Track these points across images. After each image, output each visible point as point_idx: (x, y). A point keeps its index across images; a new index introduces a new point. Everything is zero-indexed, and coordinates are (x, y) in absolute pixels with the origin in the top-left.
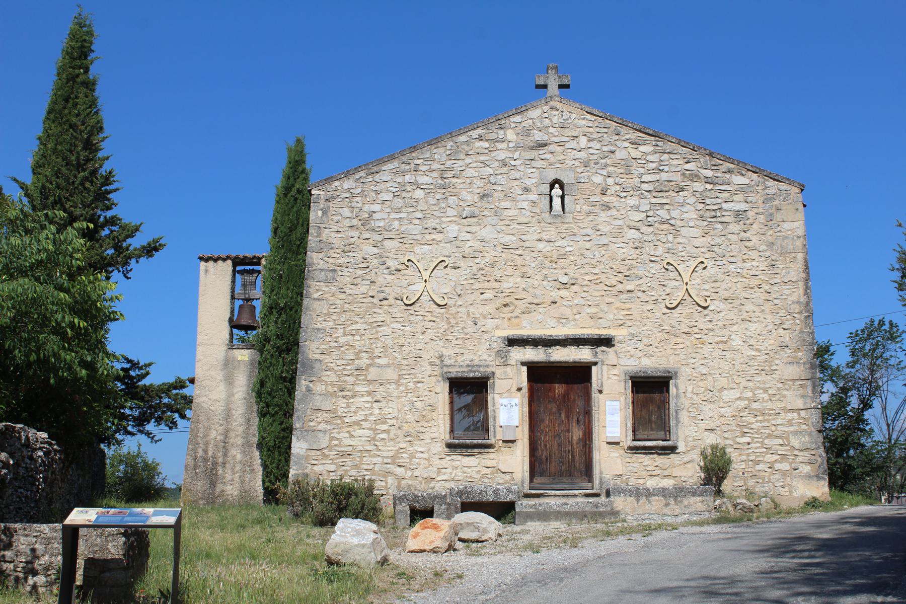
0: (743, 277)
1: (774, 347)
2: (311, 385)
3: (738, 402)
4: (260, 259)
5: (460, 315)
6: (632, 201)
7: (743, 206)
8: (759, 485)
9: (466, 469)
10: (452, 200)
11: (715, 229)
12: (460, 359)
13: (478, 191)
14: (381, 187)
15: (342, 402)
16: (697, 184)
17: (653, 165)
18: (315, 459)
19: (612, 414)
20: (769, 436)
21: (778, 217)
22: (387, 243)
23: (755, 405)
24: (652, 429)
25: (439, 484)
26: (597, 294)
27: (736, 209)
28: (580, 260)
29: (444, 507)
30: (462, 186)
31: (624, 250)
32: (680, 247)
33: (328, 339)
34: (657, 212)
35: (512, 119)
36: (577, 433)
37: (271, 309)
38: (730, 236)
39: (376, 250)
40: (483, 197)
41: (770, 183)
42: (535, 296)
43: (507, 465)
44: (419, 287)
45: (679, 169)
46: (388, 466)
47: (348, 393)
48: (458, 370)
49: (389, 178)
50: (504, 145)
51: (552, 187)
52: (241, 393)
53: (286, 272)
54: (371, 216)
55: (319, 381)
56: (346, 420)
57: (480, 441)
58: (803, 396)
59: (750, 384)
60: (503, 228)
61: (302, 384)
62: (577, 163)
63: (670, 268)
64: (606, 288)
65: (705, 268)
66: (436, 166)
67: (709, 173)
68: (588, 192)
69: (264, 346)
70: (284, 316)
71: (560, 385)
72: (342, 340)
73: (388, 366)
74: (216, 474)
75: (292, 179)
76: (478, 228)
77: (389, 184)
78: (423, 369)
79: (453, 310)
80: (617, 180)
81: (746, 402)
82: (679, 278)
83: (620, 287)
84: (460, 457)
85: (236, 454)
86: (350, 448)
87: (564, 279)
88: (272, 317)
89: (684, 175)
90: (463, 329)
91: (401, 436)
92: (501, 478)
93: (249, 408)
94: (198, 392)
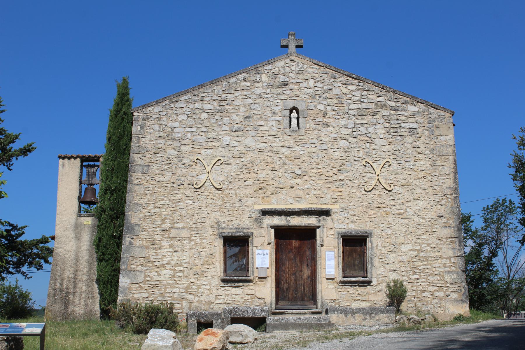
0: (414, 171)
1: (433, 217)
2: (132, 241)
3: (411, 252)
4: (99, 158)
5: (231, 195)
6: (343, 122)
7: (414, 125)
8: (425, 306)
9: (234, 296)
10: (226, 120)
11: (396, 140)
12: (230, 224)
13: (243, 114)
14: (180, 111)
15: (153, 252)
16: (385, 111)
17: (357, 98)
18: (135, 289)
19: (329, 260)
20: (431, 274)
21: (437, 132)
22: (184, 148)
23: (422, 254)
24: (355, 270)
25: (216, 306)
26: (320, 182)
27: (410, 127)
28: (309, 160)
29: (219, 321)
30: (232, 111)
31: (338, 153)
32: (374, 152)
33: (144, 211)
34: (359, 129)
35: (265, 67)
36: (306, 272)
37: (106, 190)
38: (406, 145)
39: (176, 153)
40: (246, 118)
41: (432, 110)
42: (280, 183)
43: (261, 294)
44: (204, 176)
45: (373, 101)
46: (183, 294)
47: (157, 246)
48: (229, 231)
49: (185, 105)
50: (260, 85)
51: (291, 112)
52: (85, 246)
53: (116, 167)
54: (173, 130)
55: (138, 238)
56: (156, 264)
57: (243, 278)
58: (453, 249)
59: (419, 241)
60: (259, 138)
61: (127, 240)
62: (307, 97)
63: (368, 165)
64: (326, 178)
65: (390, 165)
66: (215, 97)
67: (393, 104)
68: (314, 115)
69: (102, 215)
70: (115, 195)
71: (295, 241)
72: (153, 211)
73: (183, 228)
74: (69, 300)
75: (120, 105)
76: (243, 138)
77: (185, 109)
78: (207, 230)
79: (227, 192)
80: (334, 108)
81: (416, 252)
82: (373, 172)
83: (335, 177)
84: (230, 288)
85: (82, 286)
86: (158, 283)
87: (299, 172)
88: (107, 196)
89: (376, 105)
90: (232, 204)
91: (192, 274)
92: (257, 302)
93: (91, 256)
94: (57, 245)
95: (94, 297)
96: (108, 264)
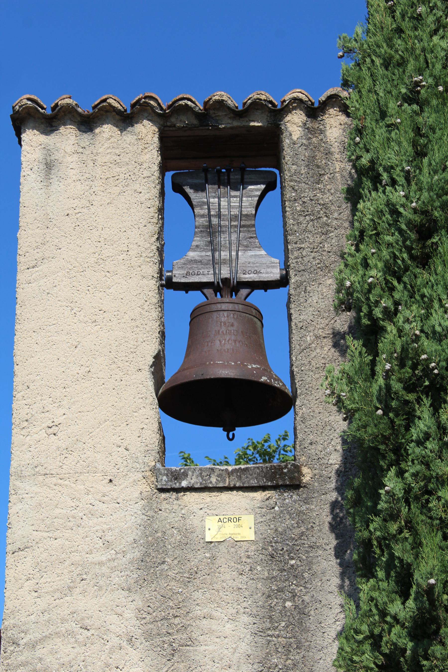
69: (411, 418)
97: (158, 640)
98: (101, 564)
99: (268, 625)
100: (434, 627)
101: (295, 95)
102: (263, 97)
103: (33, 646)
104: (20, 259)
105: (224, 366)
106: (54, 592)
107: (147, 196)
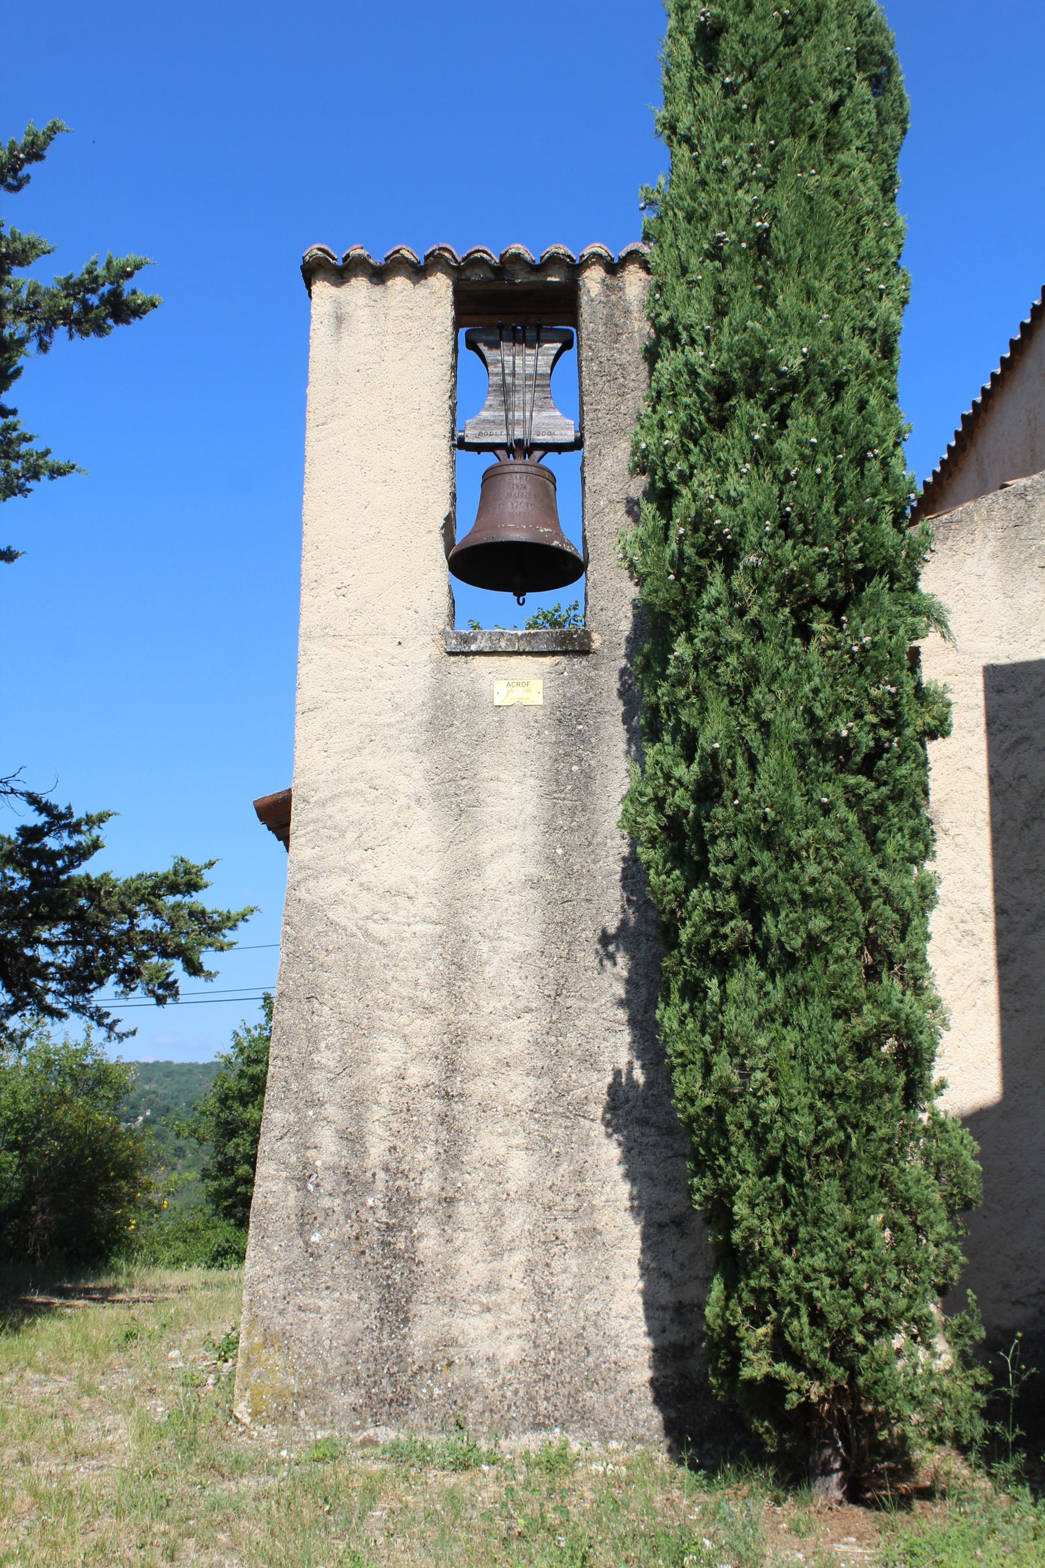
52: (513, 859)
69: (702, 584)
85: (505, 1152)
93: (559, 927)
95: (595, 1231)
96: (805, 992)
97: (446, 801)
98: (390, 725)
99: (555, 788)
100: (717, 790)
101: (594, 250)
102: (561, 251)
103: (323, 804)
104: (309, 416)
105: (515, 530)
106: (344, 752)
107: (440, 352)
